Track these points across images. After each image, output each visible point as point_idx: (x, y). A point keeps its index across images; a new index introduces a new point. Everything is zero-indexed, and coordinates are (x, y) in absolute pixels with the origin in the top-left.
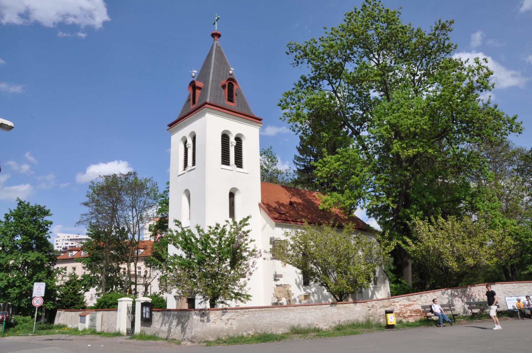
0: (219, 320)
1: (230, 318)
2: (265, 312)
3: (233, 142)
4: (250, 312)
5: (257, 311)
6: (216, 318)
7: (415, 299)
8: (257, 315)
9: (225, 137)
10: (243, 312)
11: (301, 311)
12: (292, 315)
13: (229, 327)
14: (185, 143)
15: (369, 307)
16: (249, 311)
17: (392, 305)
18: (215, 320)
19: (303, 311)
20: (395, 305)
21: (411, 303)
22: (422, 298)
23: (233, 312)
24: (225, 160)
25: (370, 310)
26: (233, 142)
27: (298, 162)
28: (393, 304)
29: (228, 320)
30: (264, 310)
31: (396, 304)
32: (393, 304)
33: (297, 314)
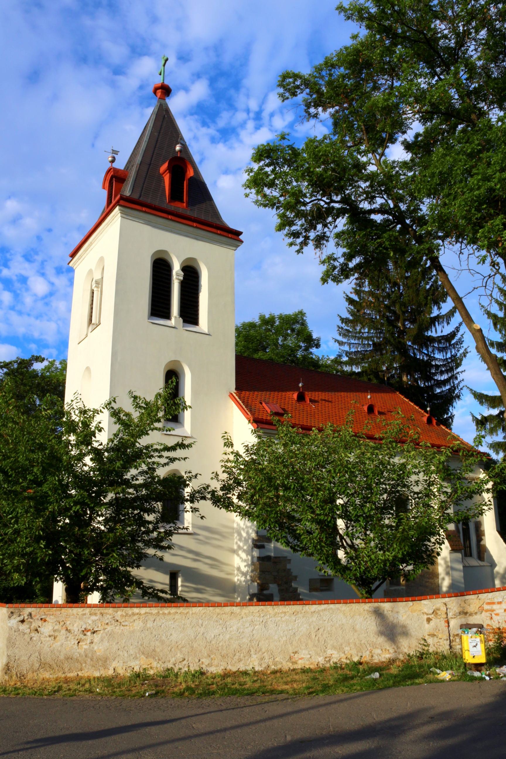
0: (63, 631)
1: (89, 628)
2: (171, 617)
4: (135, 617)
5: (151, 614)
6: (56, 627)
8: (150, 624)
10: (122, 616)
12: (235, 628)
13: (85, 649)
16: (133, 614)
18: (55, 631)
23: (95, 614)
25: (429, 620)
27: (345, 340)
29: (84, 632)
30: (169, 613)
31: (495, 607)
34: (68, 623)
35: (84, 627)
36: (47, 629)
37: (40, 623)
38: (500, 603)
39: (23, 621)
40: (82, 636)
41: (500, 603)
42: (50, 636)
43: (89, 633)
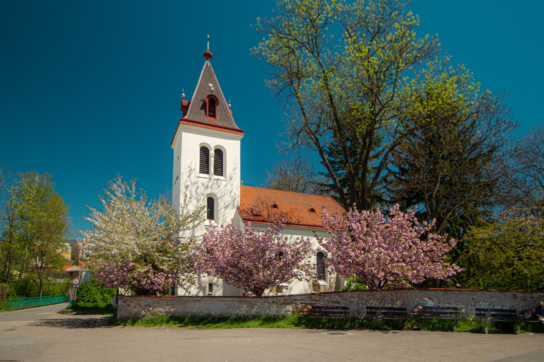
0: (138, 306)
3: (212, 153)
6: (136, 304)
7: (317, 299)
9: (204, 150)
17: (293, 303)
18: (135, 305)
20: (296, 303)
24: (204, 168)
26: (212, 153)
28: (294, 302)
29: (146, 306)
31: (297, 302)
32: (294, 302)
36: (132, 305)
37: (130, 303)
39: (124, 302)
40: (145, 308)
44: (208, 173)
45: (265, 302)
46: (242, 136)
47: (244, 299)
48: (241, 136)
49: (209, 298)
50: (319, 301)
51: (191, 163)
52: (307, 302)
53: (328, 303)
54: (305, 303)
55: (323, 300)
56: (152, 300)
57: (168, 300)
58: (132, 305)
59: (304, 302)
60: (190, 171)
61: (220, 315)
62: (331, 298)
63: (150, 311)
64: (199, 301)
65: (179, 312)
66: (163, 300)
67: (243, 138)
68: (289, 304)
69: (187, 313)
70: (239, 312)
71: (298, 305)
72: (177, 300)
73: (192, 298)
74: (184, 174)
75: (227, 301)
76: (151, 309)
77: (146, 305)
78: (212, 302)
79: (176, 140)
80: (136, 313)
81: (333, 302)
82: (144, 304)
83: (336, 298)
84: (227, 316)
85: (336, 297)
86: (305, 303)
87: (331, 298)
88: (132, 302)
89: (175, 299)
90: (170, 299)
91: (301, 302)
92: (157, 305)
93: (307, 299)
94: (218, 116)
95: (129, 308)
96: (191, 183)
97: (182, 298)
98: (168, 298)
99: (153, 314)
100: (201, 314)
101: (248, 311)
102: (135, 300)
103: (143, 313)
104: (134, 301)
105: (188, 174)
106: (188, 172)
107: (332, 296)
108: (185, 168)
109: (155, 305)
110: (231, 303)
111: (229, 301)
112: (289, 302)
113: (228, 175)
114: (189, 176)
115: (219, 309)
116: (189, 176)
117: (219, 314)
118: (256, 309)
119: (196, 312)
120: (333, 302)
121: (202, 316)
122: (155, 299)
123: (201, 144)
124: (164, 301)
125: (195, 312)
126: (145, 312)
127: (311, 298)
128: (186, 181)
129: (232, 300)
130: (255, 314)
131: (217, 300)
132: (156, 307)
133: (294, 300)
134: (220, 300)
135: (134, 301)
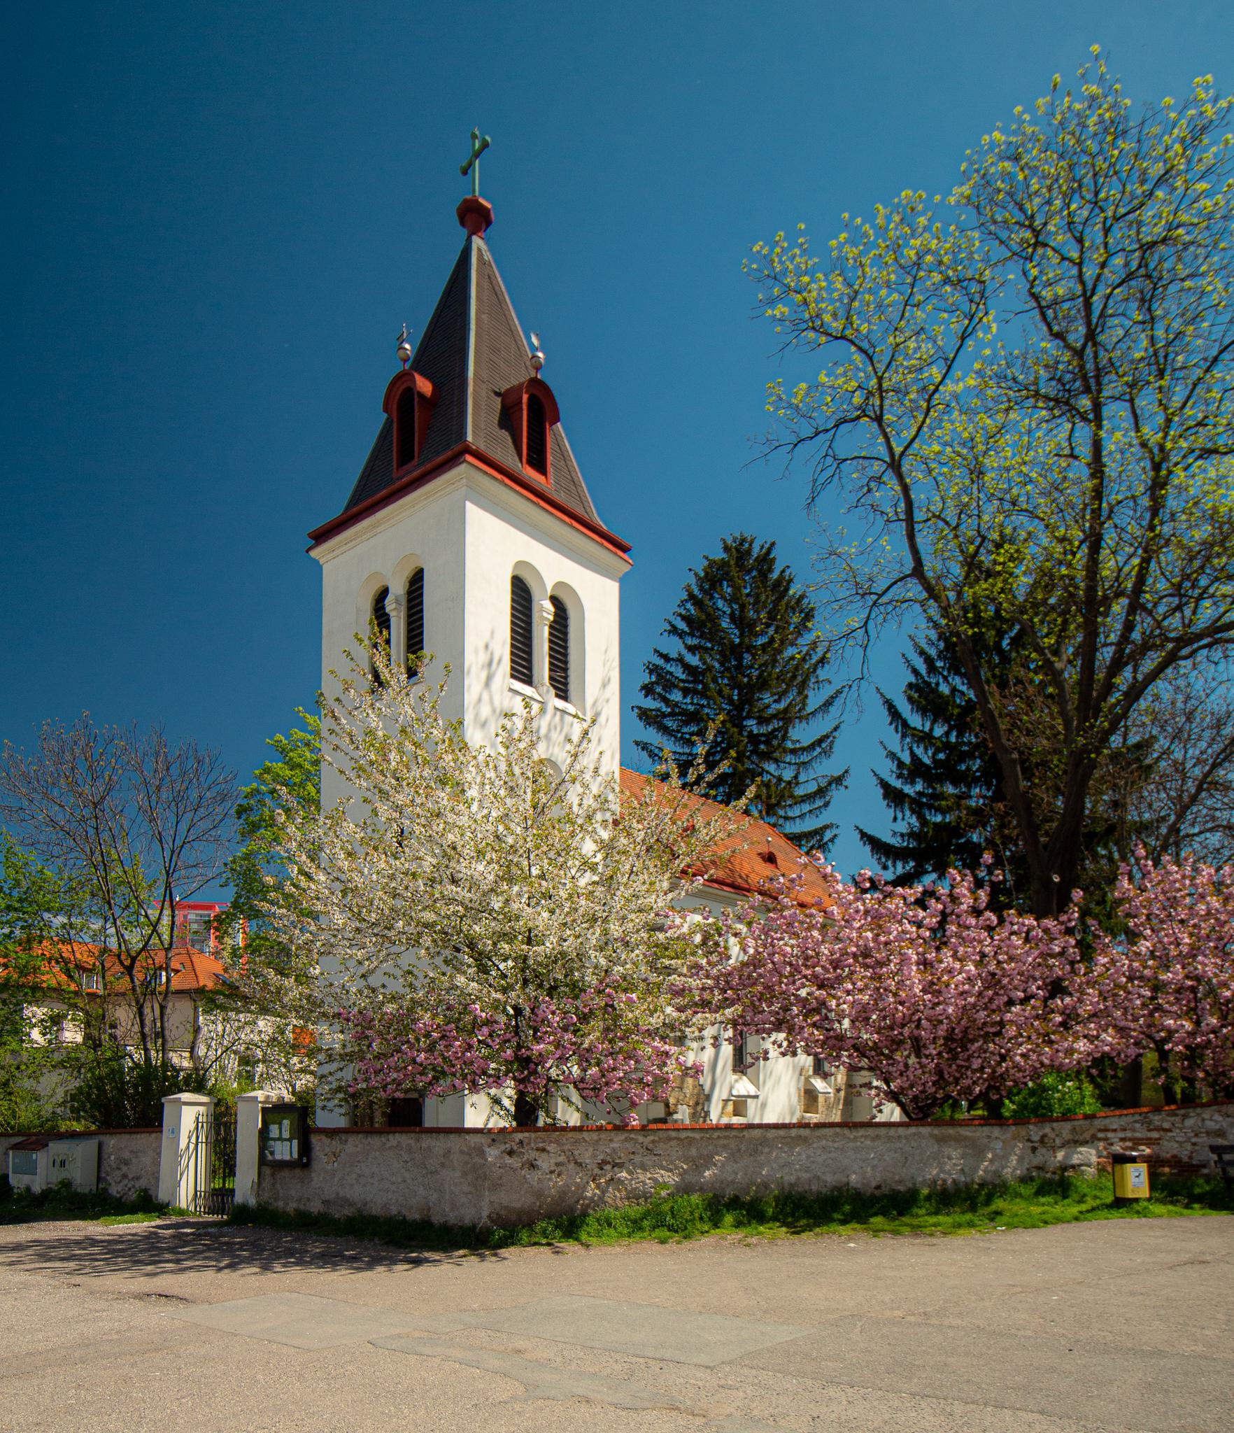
0: (572, 1166)
1: (608, 1158)
6: (562, 1159)
7: (1166, 1125)
10: (653, 1141)
11: (830, 1144)
14: (384, 593)
15: (1032, 1142)
17: (1100, 1139)
18: (557, 1164)
19: (836, 1145)
20: (1106, 1139)
21: (1155, 1135)
22: (1189, 1122)
28: (1100, 1135)
31: (1110, 1135)
33: (819, 1152)
34: (576, 1153)
35: (601, 1157)
36: (545, 1163)
38: (1115, 1130)
39: (511, 1153)
40: (597, 1171)
41: (1115, 1130)
42: (552, 1172)
43: (608, 1167)
44: (528, 680)
45: (1014, 1139)
46: (627, 568)
47: (951, 1131)
48: (621, 566)
49: (838, 1130)
50: (1169, 1130)
51: (492, 633)
52: (1138, 1135)
53: (1196, 1135)
54: (1130, 1140)
55: (1181, 1129)
56: (626, 1140)
57: (691, 1141)
58: (545, 1163)
59: (1129, 1134)
60: (490, 664)
61: (878, 1187)
62: (1203, 1120)
63: (620, 1181)
64: (805, 1140)
65: (733, 1182)
66: (670, 1139)
67: (626, 574)
68: (1087, 1142)
69: (766, 1186)
70: (938, 1174)
71: (1112, 1144)
72: (726, 1137)
73: (782, 1132)
74: (473, 670)
75: (899, 1137)
76: (624, 1174)
77: (604, 1162)
78: (851, 1144)
79: (374, 526)
80: (563, 1193)
81: (1208, 1133)
82: (594, 1156)
83: (1216, 1121)
84: (902, 1188)
85: (1217, 1117)
86: (1130, 1140)
87: (1203, 1120)
88: (543, 1150)
89: (716, 1134)
90: (697, 1136)
91: (1122, 1135)
92: (648, 1160)
93: (1138, 1125)
94: (550, 469)
95: (533, 1177)
96: (494, 711)
97: (745, 1133)
98: (690, 1134)
99: (634, 1196)
100: (814, 1188)
101: (966, 1169)
102: (557, 1142)
103: (591, 1191)
104: (552, 1148)
105: (484, 675)
106: (483, 667)
107: (1206, 1116)
108: (476, 651)
109: (637, 1159)
110: (913, 1144)
111: (906, 1137)
112: (1087, 1136)
113: (589, 701)
114: (488, 683)
115: (874, 1167)
116: (488, 683)
117: (874, 1184)
118: (991, 1161)
119: (798, 1178)
120: (1208, 1133)
121: (819, 1193)
122: (641, 1139)
123: (520, 564)
124: (674, 1143)
125: (793, 1179)
126: (598, 1186)
127: (1150, 1122)
128: (480, 700)
129: (914, 1134)
130: (989, 1178)
131: (866, 1137)
132: (644, 1168)
133: (1100, 1130)
134: (878, 1137)
135: (552, 1148)
